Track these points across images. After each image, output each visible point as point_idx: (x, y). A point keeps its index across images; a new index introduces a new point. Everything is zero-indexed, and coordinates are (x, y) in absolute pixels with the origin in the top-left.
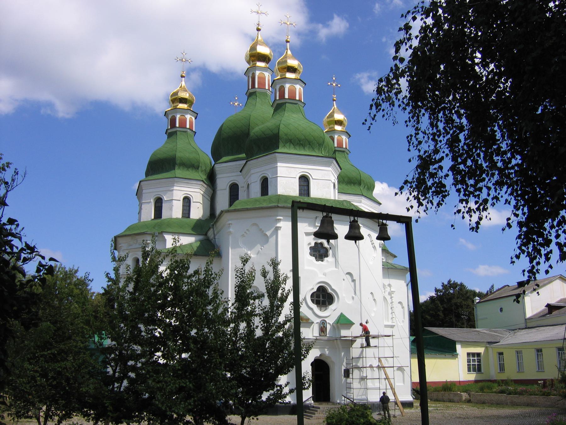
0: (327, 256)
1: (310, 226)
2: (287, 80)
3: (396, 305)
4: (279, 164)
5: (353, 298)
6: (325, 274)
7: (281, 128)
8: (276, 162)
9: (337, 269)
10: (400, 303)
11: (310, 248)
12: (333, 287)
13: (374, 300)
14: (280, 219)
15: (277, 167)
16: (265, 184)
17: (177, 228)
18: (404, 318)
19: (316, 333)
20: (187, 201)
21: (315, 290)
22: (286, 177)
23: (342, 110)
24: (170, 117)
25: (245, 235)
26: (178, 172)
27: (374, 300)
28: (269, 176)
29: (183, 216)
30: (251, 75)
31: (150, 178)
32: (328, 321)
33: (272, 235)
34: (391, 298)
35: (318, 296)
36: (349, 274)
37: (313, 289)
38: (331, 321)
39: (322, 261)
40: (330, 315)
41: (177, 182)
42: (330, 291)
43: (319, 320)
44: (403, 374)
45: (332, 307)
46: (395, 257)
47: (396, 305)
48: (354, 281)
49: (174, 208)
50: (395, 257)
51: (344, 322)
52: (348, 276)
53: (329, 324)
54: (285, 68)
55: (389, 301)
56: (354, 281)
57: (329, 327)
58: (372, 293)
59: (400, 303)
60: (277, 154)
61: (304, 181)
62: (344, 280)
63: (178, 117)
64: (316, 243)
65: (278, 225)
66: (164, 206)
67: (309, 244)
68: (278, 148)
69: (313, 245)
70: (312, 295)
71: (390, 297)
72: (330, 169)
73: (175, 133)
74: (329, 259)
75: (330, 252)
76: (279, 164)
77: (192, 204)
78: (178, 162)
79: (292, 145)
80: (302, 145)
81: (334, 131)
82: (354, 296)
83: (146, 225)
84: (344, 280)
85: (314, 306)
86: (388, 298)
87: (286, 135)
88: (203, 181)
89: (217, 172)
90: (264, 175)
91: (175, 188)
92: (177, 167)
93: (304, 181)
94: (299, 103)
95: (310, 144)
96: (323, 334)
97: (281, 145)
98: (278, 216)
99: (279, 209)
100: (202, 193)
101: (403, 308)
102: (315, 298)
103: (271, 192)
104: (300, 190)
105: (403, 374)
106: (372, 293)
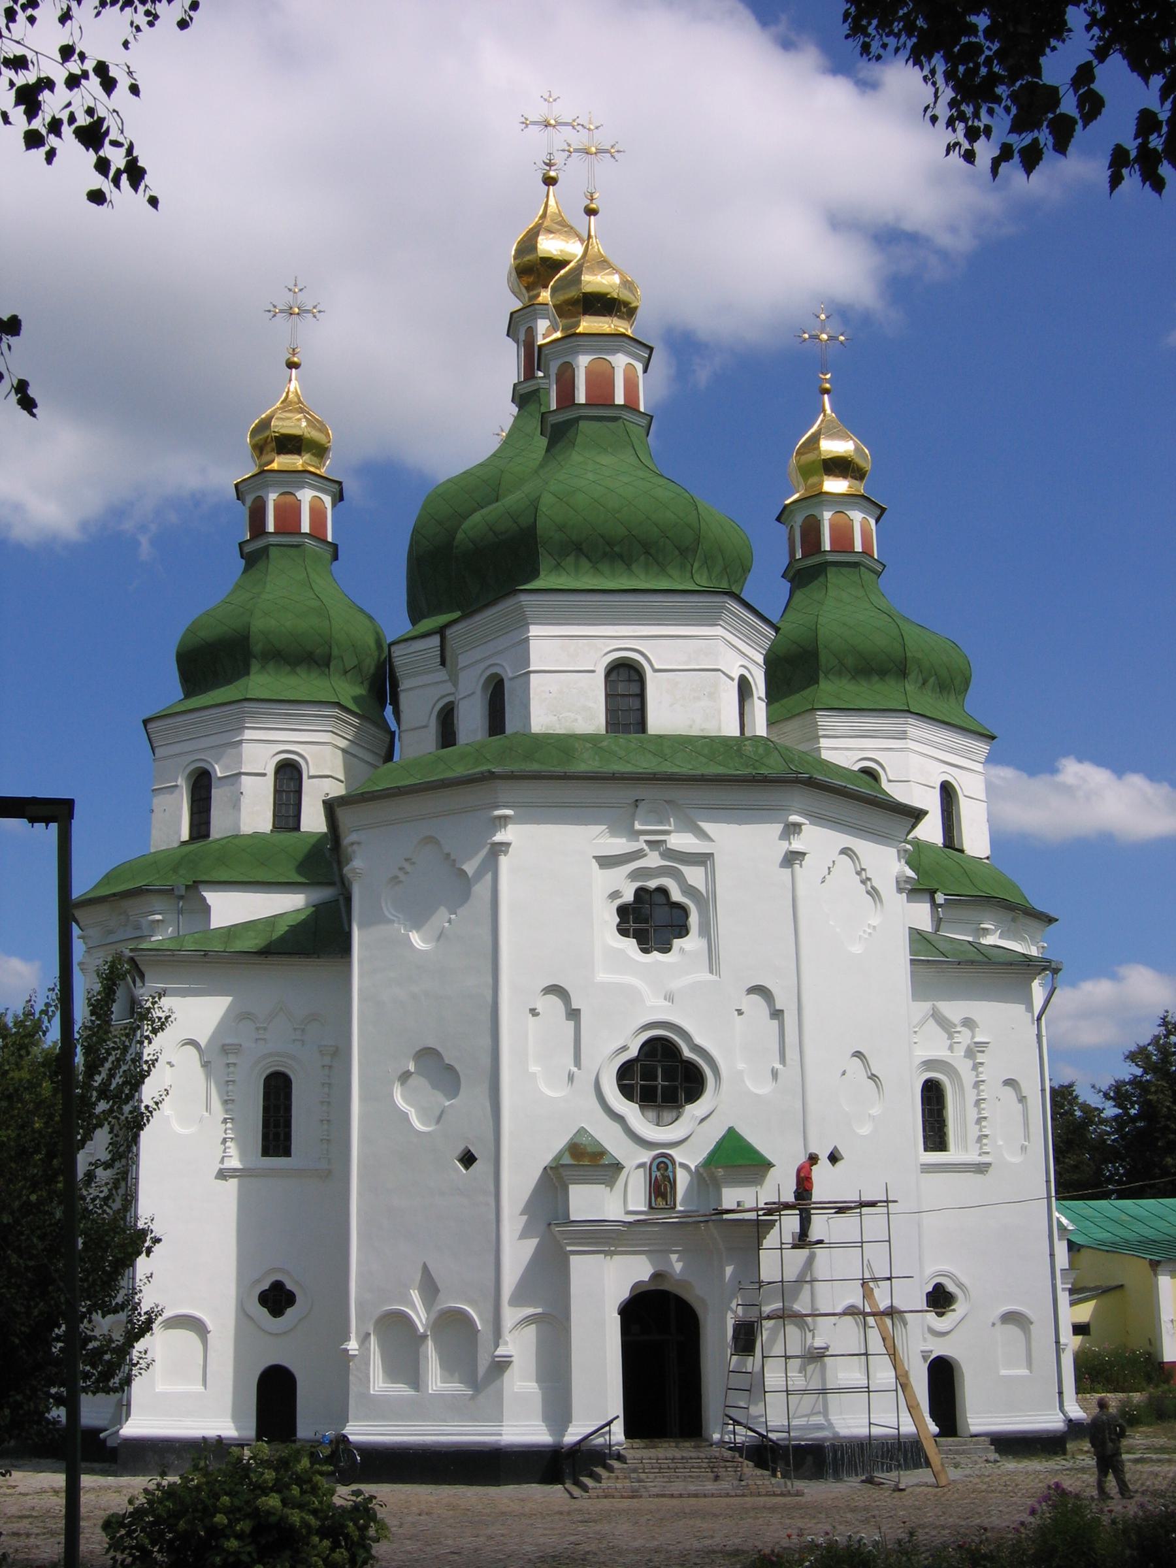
0: (682, 930)
1: (614, 831)
2: (582, 341)
3: (993, 1089)
4: (534, 630)
5: (775, 1074)
6: (670, 997)
7: (543, 508)
8: (523, 623)
9: (713, 977)
10: (1010, 1082)
11: (622, 911)
12: (698, 1040)
13: (873, 1077)
14: (506, 817)
15: (527, 639)
16: (498, 699)
17: (249, 866)
18: (1027, 1137)
19: (638, 1201)
20: (289, 775)
21: (633, 1052)
22: (561, 672)
23: (848, 423)
24: (249, 502)
25: (402, 877)
26: (259, 682)
27: (873, 1077)
28: (508, 673)
29: (276, 827)
32: (679, 1159)
33: (479, 874)
34: (976, 1066)
35: (648, 1074)
36: (759, 990)
37: (624, 1048)
38: (689, 1158)
40: (691, 1134)
41: (254, 715)
42: (687, 1053)
43: (646, 1156)
44: (205, 1342)
45: (694, 1110)
46: (1051, 920)
47: (993, 1089)
48: (777, 1014)
49: (245, 802)
50: (1051, 920)
51: (737, 1158)
52: (756, 998)
53: (684, 1166)
54: (573, 302)
55: (968, 1077)
56: (777, 1014)
57: (682, 1180)
58: (858, 1054)
59: (1010, 1082)
60: (523, 598)
61: (626, 678)
62: (740, 1012)
64: (640, 893)
65: (499, 837)
66: (218, 795)
67: (615, 895)
68: (534, 574)
69: (628, 897)
70: (625, 1072)
71: (970, 1063)
72: (718, 631)
73: (265, 550)
74: (690, 945)
75: (694, 919)
78: (257, 648)
79: (584, 562)
80: (621, 556)
81: (819, 497)
82: (778, 1066)
83: (154, 862)
84: (740, 1012)
85: (630, 1110)
86: (964, 1067)
87: (561, 528)
88: (338, 705)
89: (400, 672)
91: (248, 734)
92: (255, 666)
93: (626, 678)
94: (626, 415)
95: (647, 553)
96: (662, 1204)
97: (545, 563)
98: (497, 807)
100: (343, 744)
101: (1022, 1099)
102: (638, 1082)
103: (510, 728)
104: (611, 712)
105: (205, 1342)
106: (858, 1054)
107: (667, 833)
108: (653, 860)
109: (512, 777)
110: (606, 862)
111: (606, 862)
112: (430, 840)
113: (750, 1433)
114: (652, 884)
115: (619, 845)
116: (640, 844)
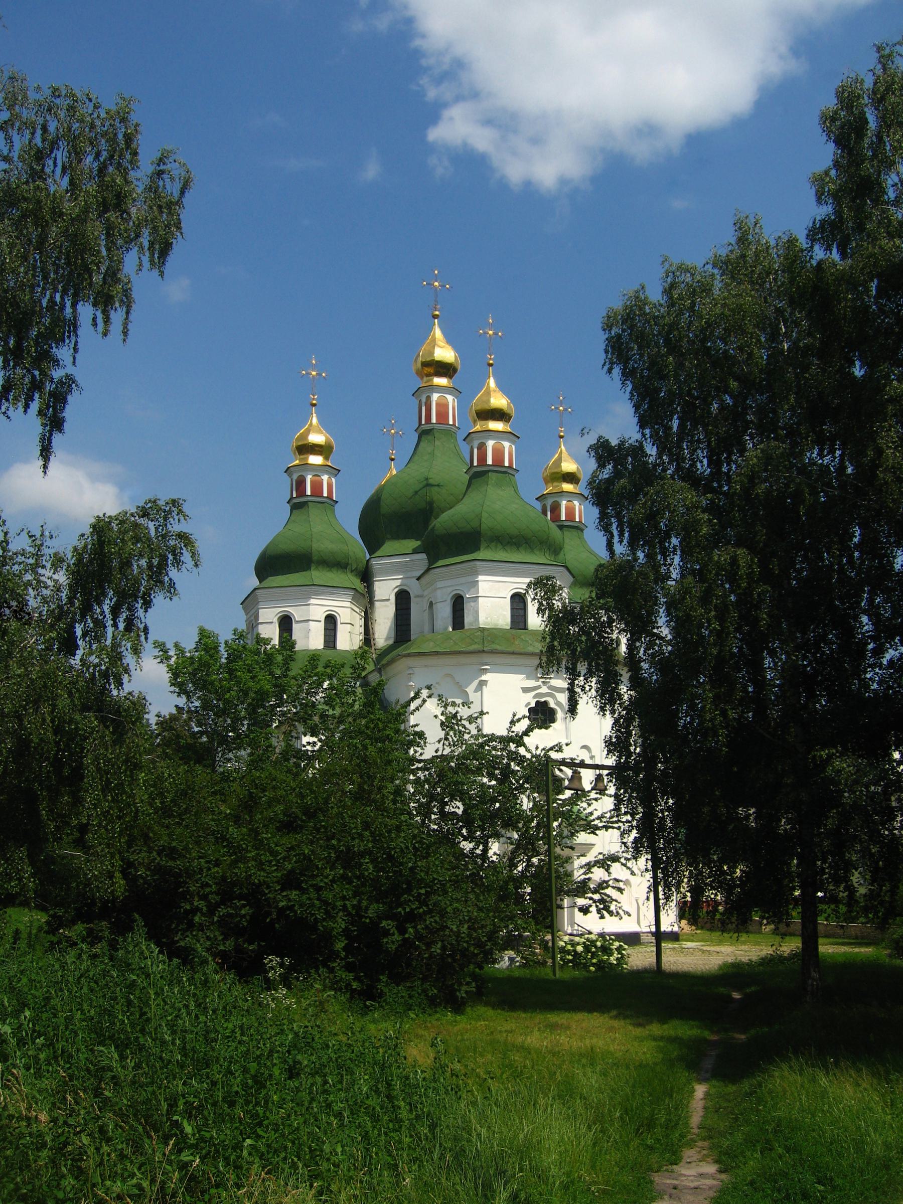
7: (483, 520)
16: (458, 604)
20: (331, 621)
24: (295, 477)
30: (424, 400)
31: (266, 583)
39: (546, 728)
49: (312, 635)
63: (309, 478)
64: (537, 702)
65: (484, 678)
67: (529, 704)
69: (533, 705)
76: (480, 578)
77: (340, 627)
78: (315, 558)
79: (500, 546)
80: (515, 544)
90: (462, 593)
91: (312, 601)
99: (484, 655)
103: (468, 619)
107: (550, 678)
108: (544, 690)
109: (493, 652)
110: (526, 690)
111: (526, 690)
112: (449, 675)
113: (580, 928)
114: (543, 700)
115: (532, 683)
116: (540, 683)
